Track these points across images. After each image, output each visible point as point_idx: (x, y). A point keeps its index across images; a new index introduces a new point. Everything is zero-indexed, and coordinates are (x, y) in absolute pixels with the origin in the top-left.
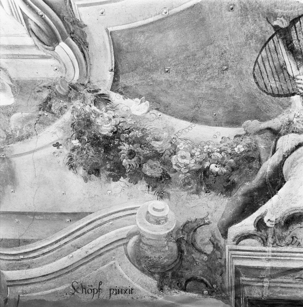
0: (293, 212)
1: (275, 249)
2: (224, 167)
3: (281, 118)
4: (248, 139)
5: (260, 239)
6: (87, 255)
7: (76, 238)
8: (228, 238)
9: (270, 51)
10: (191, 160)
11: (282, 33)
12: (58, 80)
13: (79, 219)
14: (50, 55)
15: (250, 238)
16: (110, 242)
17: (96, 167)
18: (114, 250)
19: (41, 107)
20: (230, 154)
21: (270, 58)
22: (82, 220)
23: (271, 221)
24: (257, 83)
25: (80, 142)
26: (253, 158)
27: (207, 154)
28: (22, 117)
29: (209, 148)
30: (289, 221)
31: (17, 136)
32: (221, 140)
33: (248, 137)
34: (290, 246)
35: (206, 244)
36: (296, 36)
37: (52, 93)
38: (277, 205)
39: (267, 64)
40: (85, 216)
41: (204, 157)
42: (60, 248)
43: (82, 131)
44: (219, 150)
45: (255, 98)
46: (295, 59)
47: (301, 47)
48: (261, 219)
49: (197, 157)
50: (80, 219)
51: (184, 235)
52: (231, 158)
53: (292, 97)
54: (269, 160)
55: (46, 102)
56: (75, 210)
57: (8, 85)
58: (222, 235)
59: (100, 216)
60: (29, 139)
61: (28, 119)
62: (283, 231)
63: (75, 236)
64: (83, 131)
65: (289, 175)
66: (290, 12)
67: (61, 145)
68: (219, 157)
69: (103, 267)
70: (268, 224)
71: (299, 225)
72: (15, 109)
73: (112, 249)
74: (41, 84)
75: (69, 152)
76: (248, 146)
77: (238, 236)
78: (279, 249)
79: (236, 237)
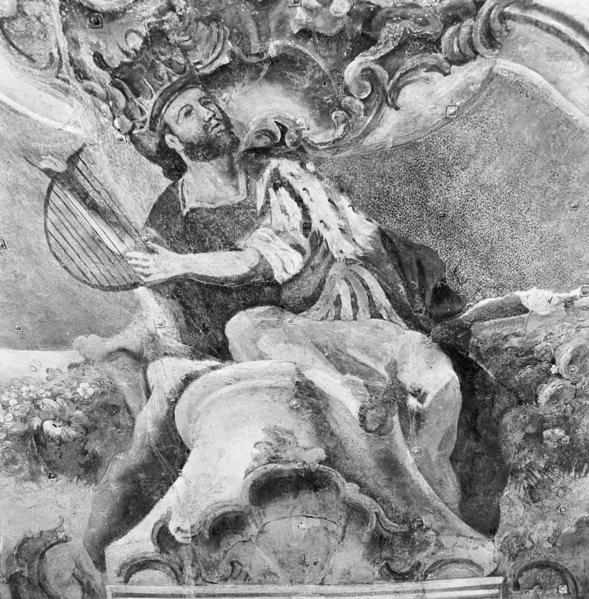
0: (220, 512)
1: (200, 590)
2: (70, 426)
3: (135, 329)
4: (93, 372)
5: (168, 569)
8: (108, 570)
9: (60, 211)
10: (6, 414)
11: (63, 181)
15: (148, 568)
20: (72, 400)
21: (67, 224)
23: (182, 531)
24: (66, 268)
26: (115, 406)
27: (30, 402)
29: (30, 391)
30: (219, 529)
32: (47, 375)
33: (92, 368)
34: (229, 581)
35: (68, 584)
36: (89, 185)
38: (188, 497)
39: (66, 234)
41: (28, 409)
44: (49, 394)
45: (75, 294)
46: (107, 223)
47: (108, 203)
48: (163, 527)
49: (13, 408)
51: (22, 566)
52: (77, 408)
53: (135, 290)
54: (145, 408)
58: (94, 562)
62: (210, 551)
65: (191, 439)
66: (58, 145)
68: (55, 406)
70: (179, 537)
71: (239, 538)
76: (98, 383)
77: (125, 564)
78: (209, 589)
79: (122, 567)
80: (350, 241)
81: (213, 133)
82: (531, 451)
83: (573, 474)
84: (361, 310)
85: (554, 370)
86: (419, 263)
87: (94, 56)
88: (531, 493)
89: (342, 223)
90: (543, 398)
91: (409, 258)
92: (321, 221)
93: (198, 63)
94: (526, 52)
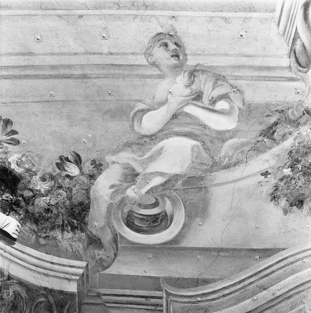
6: (273, 297)
7: (262, 278)
12: (294, 104)
13: (269, 256)
14: (300, 78)
16: (302, 283)
17: (301, 198)
18: (304, 292)
19: (263, 132)
22: (272, 257)
25: (293, 171)
28: (238, 143)
31: (224, 164)
37: (282, 117)
40: (276, 253)
42: (243, 289)
43: (298, 159)
50: (271, 256)
55: (271, 128)
56: (267, 246)
57: (238, 109)
59: (294, 252)
60: (237, 167)
61: (243, 145)
63: (262, 276)
64: (299, 160)
67: (270, 174)
69: (291, 311)
72: (234, 133)
73: (303, 291)
74: (274, 108)
75: (276, 181)
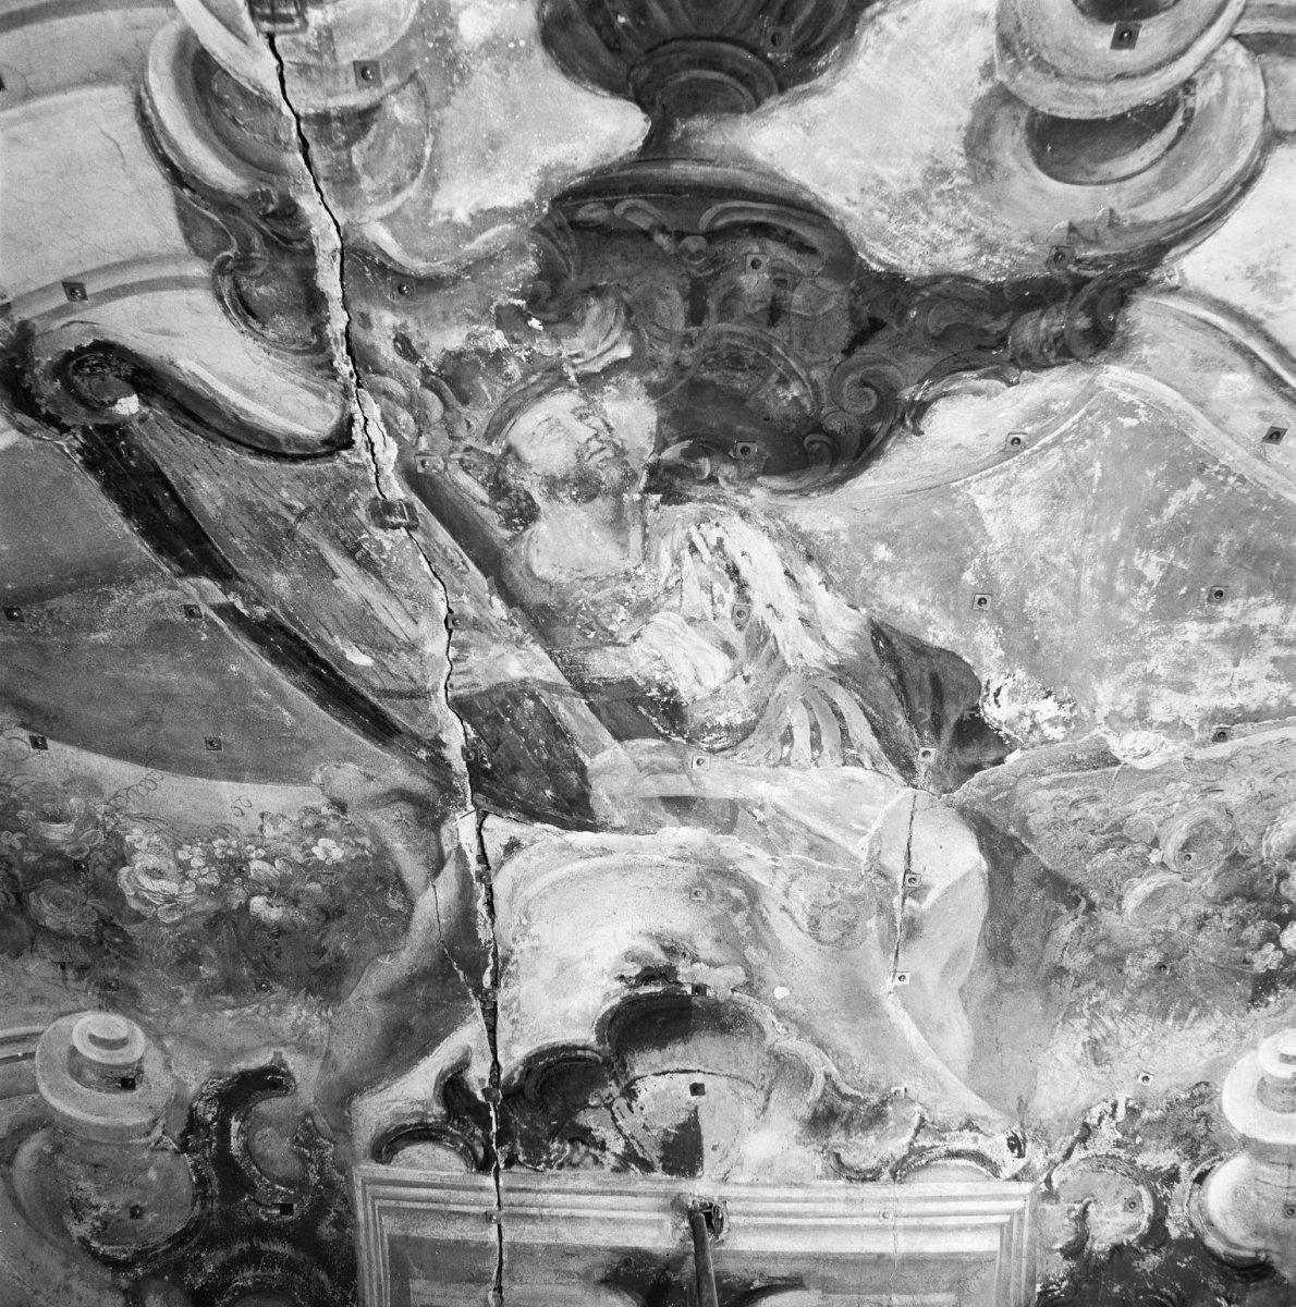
52: (311, 879)
80: (816, 639)
81: (591, 462)
82: (1101, 984)
83: (1170, 1022)
84: (826, 751)
85: (1154, 858)
86: (935, 680)
87: (395, 340)
88: (1093, 1050)
89: (805, 609)
90: (1130, 904)
91: (918, 670)
92: (770, 606)
93: (577, 356)
94: (1154, 357)
